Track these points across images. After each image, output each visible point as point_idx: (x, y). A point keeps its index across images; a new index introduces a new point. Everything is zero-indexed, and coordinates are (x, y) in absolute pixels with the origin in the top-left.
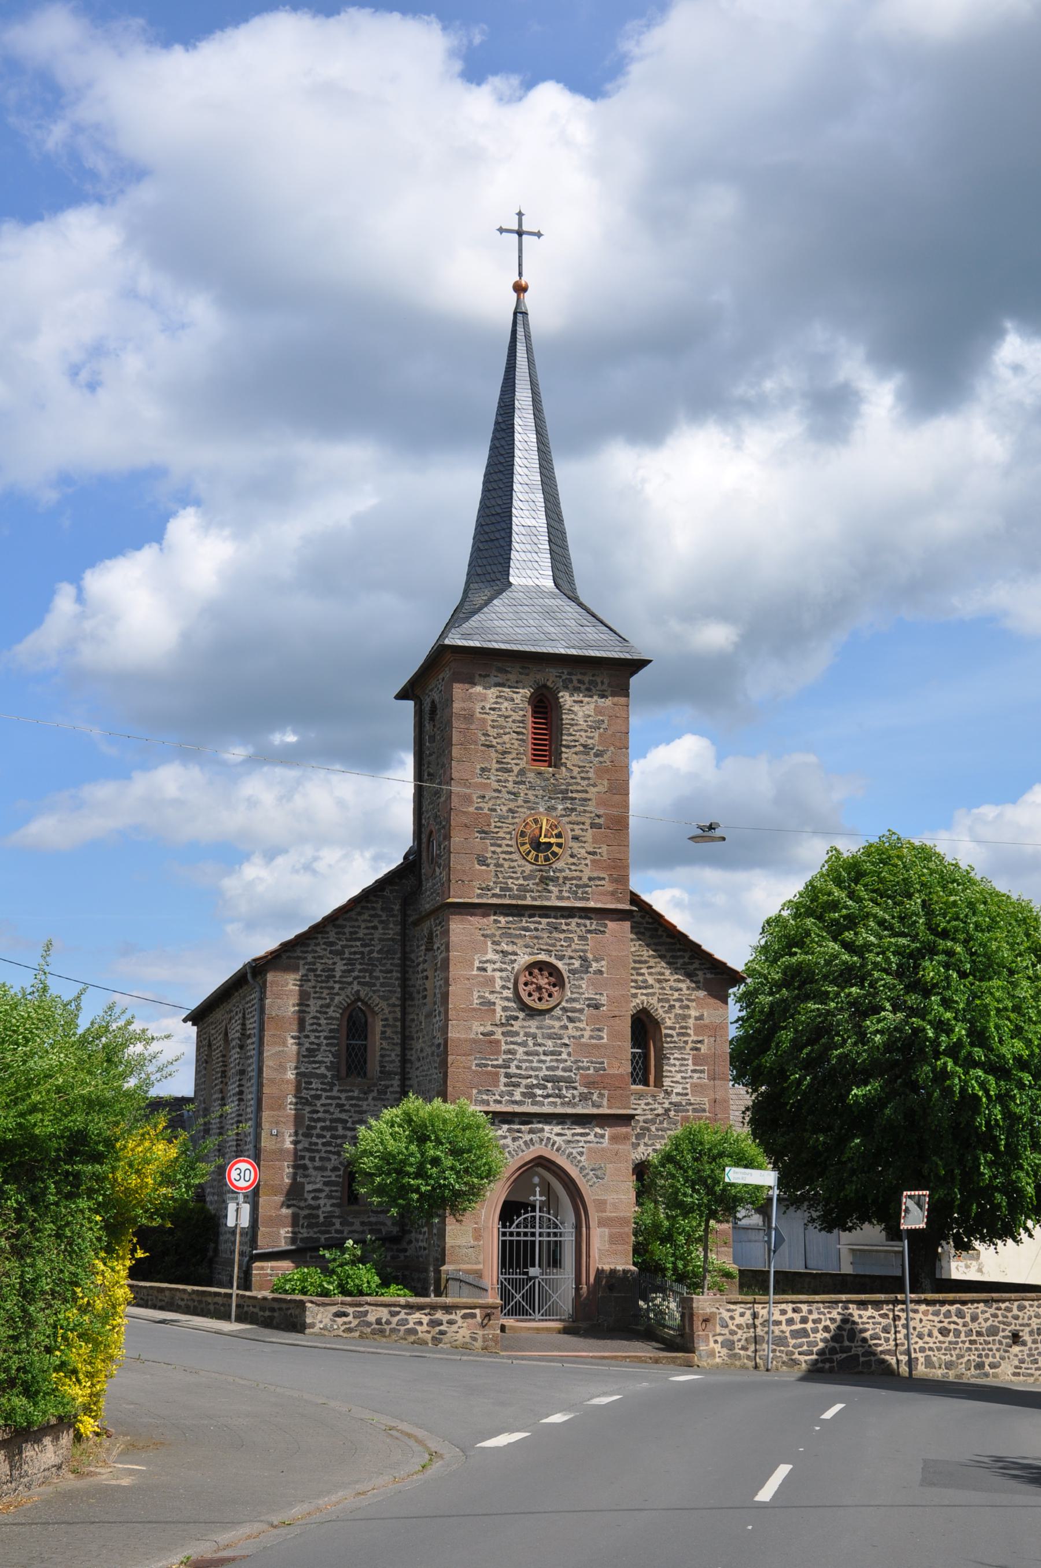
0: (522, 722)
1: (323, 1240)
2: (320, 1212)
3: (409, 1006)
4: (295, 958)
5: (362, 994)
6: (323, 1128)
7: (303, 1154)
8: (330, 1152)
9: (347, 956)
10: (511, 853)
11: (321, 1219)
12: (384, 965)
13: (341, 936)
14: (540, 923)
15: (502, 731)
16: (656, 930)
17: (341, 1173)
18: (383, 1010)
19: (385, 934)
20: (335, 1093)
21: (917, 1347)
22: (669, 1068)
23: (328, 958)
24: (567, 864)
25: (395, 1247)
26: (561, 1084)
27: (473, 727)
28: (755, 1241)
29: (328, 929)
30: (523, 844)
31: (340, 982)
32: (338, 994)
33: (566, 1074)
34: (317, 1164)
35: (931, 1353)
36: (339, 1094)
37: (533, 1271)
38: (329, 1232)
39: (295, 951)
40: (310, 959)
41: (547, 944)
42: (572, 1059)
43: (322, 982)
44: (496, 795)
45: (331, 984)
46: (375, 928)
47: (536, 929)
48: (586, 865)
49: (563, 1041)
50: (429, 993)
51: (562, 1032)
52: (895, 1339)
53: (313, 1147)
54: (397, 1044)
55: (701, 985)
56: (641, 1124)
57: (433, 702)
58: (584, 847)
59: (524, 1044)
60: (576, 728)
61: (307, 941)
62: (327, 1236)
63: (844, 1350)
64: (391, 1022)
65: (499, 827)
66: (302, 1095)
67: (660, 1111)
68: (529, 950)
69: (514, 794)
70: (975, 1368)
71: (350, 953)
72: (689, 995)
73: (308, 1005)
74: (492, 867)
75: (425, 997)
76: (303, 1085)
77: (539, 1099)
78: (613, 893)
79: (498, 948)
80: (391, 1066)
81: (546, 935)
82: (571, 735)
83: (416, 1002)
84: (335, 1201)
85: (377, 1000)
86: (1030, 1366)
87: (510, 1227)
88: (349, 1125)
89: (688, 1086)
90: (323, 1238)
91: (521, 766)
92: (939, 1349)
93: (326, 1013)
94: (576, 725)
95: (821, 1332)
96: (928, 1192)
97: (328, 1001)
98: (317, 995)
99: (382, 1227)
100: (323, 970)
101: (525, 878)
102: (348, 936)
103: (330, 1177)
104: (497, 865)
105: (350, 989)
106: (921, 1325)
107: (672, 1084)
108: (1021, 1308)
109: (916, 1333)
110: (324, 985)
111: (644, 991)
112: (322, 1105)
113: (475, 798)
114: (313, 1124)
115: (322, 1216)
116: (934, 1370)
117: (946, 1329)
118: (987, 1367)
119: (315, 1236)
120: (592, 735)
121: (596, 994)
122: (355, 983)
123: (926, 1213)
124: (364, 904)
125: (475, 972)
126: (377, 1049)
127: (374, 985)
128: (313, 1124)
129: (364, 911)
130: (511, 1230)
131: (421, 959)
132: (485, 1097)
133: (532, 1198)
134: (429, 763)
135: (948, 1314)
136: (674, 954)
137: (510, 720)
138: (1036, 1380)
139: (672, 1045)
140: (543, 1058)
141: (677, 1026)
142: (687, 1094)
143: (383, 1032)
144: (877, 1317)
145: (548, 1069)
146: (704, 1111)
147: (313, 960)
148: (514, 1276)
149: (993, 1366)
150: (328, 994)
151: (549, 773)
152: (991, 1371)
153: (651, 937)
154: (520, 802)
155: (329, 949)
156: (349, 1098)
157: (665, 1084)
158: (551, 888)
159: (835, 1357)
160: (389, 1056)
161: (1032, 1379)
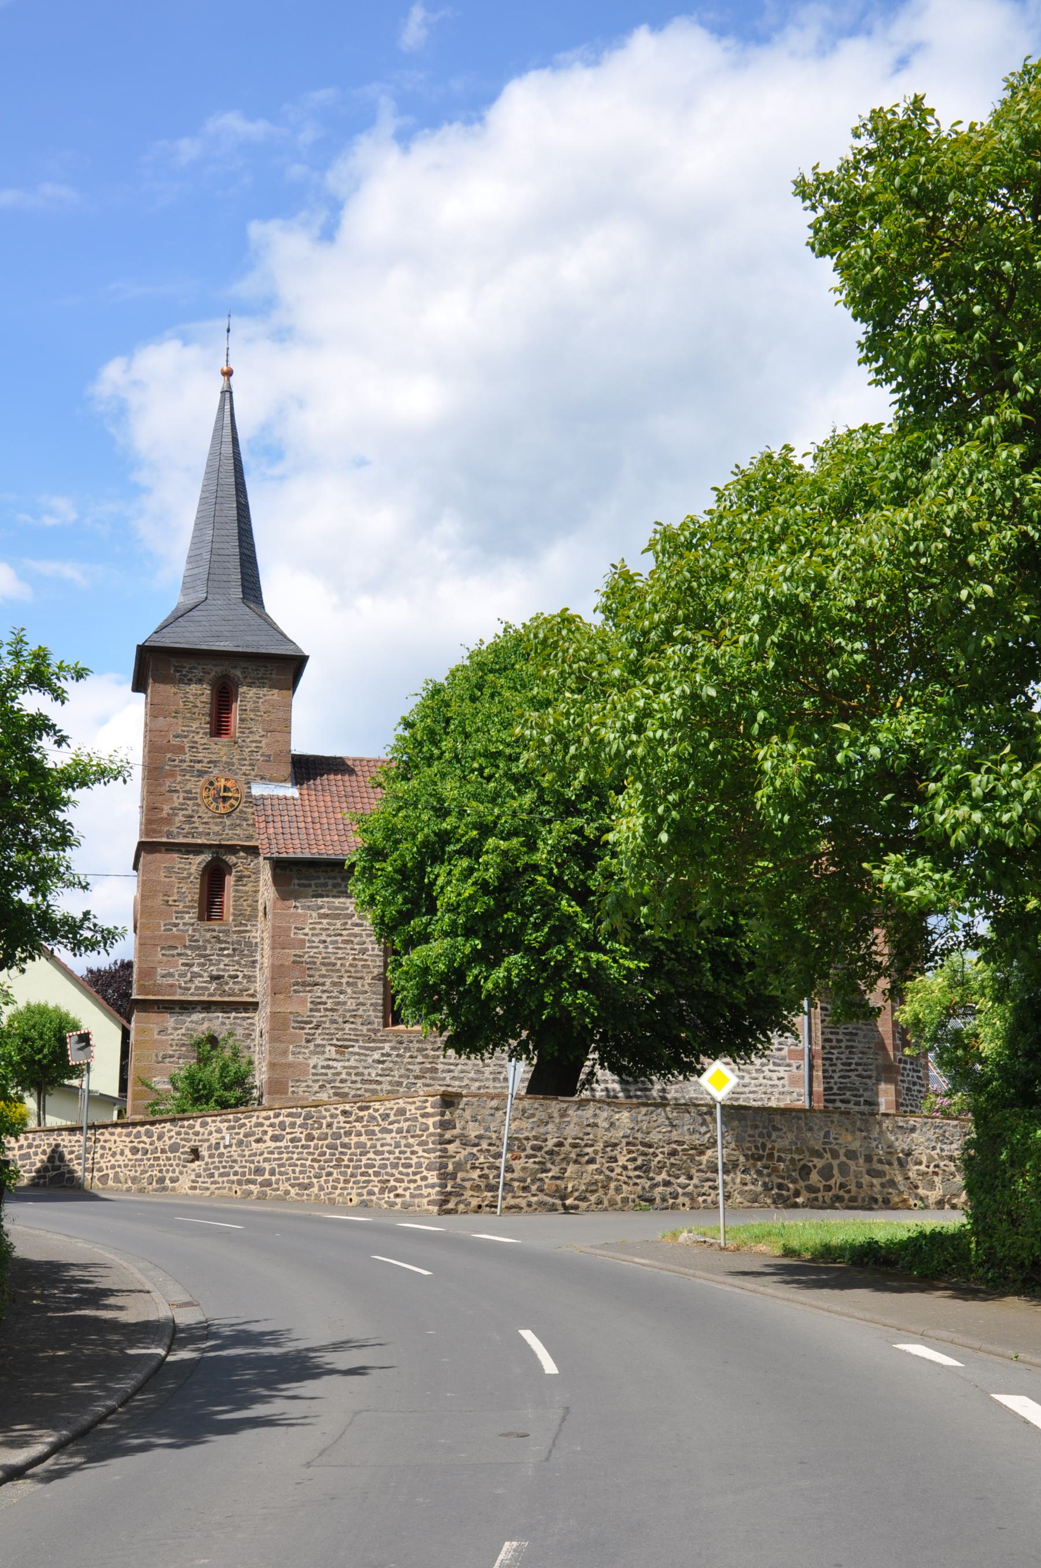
21: (109, 1165)
52: (93, 1159)
63: (54, 1169)
70: (157, 1183)
86: (206, 1180)
92: (126, 1166)
108: (204, 1125)
117: (135, 1147)
118: (167, 1182)
135: (138, 1135)
138: (212, 1193)
149: (174, 1180)
152: (170, 1185)
159: (48, 1174)
161: (208, 1193)
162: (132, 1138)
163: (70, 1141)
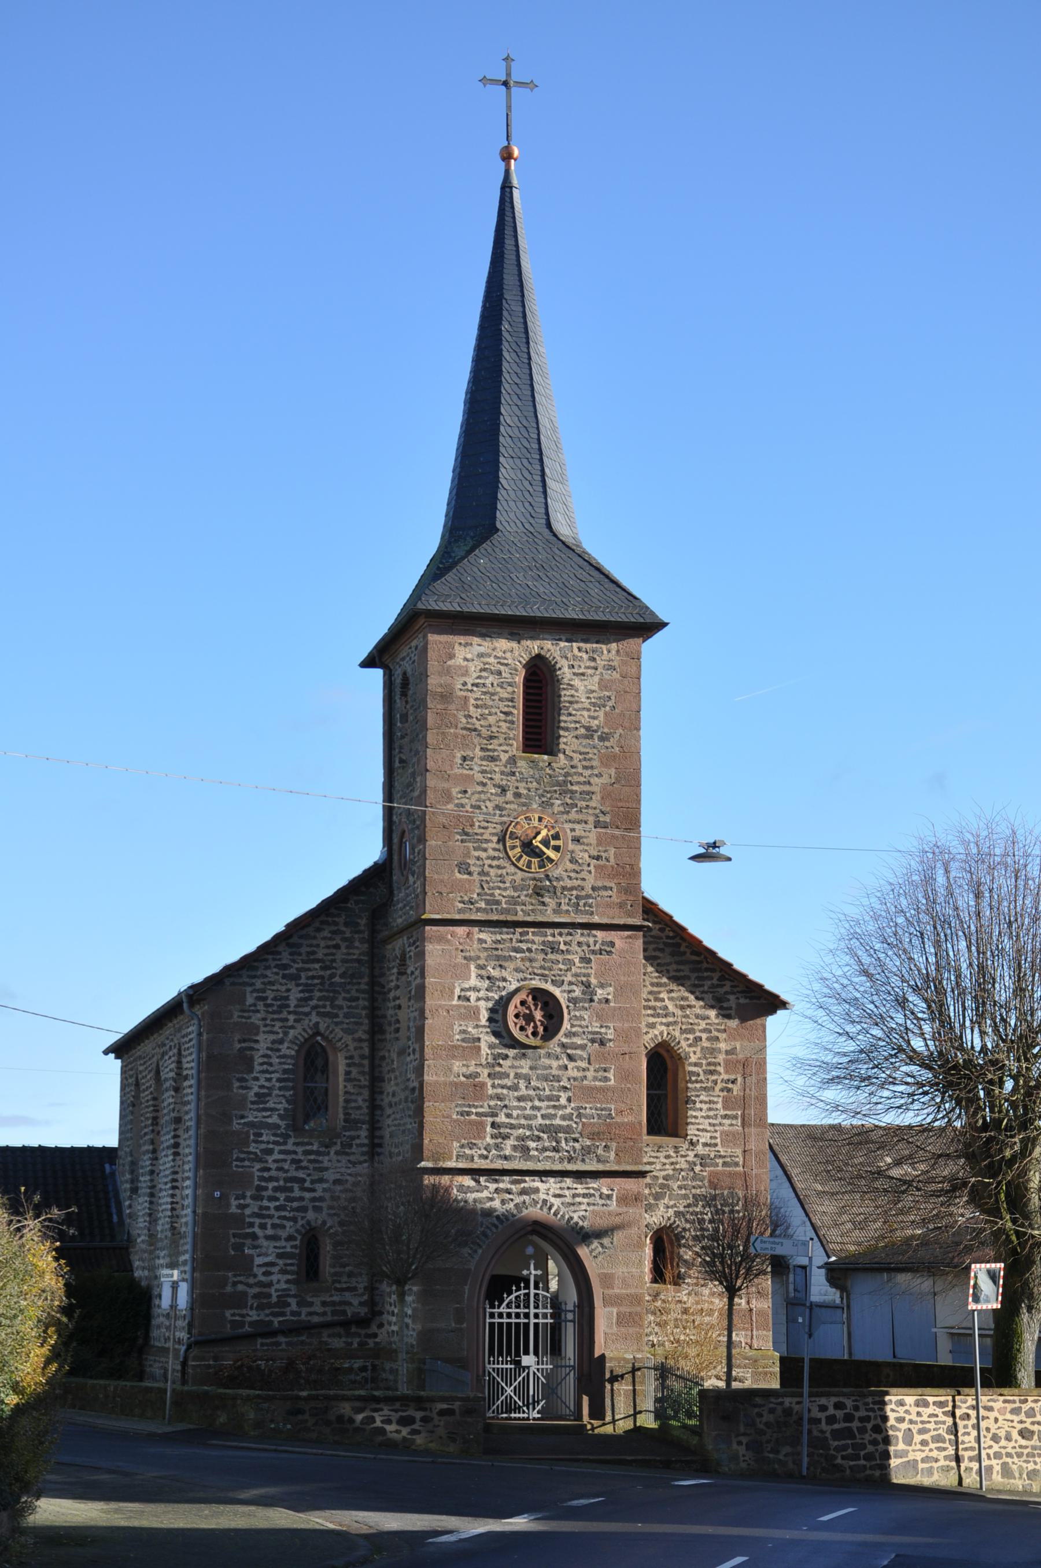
0: (512, 700)
1: (276, 1324)
2: (273, 1291)
3: (379, 1040)
4: (240, 984)
5: (322, 1027)
6: (276, 1189)
7: (252, 1220)
8: (284, 1218)
9: (303, 981)
10: (499, 858)
11: (274, 1299)
12: (348, 992)
13: (296, 957)
14: (533, 942)
15: (487, 712)
16: (679, 945)
17: (298, 1242)
18: (347, 1046)
19: (349, 954)
20: (289, 1147)
21: (991, 1452)
22: (694, 1114)
23: (281, 984)
24: (566, 871)
25: (363, 1332)
26: (560, 1135)
27: (452, 707)
28: (831, 1323)
29: (280, 948)
30: (513, 848)
31: (295, 1013)
32: (292, 1027)
33: (565, 1123)
34: (270, 1232)
35: (1009, 1460)
36: (294, 1148)
37: (528, 1360)
38: (283, 1314)
39: (241, 976)
40: (259, 985)
41: (542, 967)
42: (573, 1105)
43: (273, 1013)
44: (480, 788)
45: (284, 1015)
46: (337, 947)
47: (529, 950)
48: (590, 872)
49: (562, 1084)
50: (403, 1025)
51: (560, 1073)
53: (264, 1212)
54: (364, 1087)
55: (733, 1012)
56: (661, 1181)
57: (405, 673)
58: (586, 851)
59: (515, 1088)
60: (576, 706)
61: (256, 964)
62: (281, 1319)
64: (357, 1060)
65: (483, 828)
66: (251, 1149)
67: (684, 1166)
68: (520, 975)
69: (499, 786)
71: (308, 978)
72: (718, 1024)
73: (257, 1041)
74: (476, 876)
75: (397, 1030)
76: (252, 1137)
77: (532, 1153)
78: (621, 905)
79: (483, 973)
80: (358, 1112)
81: (541, 956)
82: (570, 715)
83: (388, 1036)
84: (290, 1277)
85: (341, 1034)
87: (499, 1307)
88: (307, 1185)
89: (718, 1135)
90: (276, 1321)
91: (510, 754)
93: (279, 1050)
94: (577, 702)
95: (870, 1432)
96: (1003, 1265)
97: (281, 1035)
98: (268, 1029)
99: (347, 1308)
100: (275, 999)
101: (515, 889)
102: (304, 957)
103: (285, 1247)
104: (482, 873)
105: (307, 1022)
106: (996, 1426)
107: (697, 1133)
109: (990, 1435)
110: (275, 1016)
111: (664, 1020)
112: (275, 1161)
113: (454, 794)
114: (263, 1184)
115: (274, 1295)
116: (1012, 1481)
119: (267, 1319)
120: (596, 714)
121: (601, 1027)
122: (314, 1013)
123: (1001, 1290)
124: (323, 918)
125: (455, 1002)
126: (341, 1093)
127: (337, 1016)
128: (263, 1184)
129: (325, 927)
130: (501, 1310)
131: (393, 984)
132: (468, 1151)
133: (525, 1272)
134: (401, 747)
136: (700, 974)
137: (496, 697)
139: (698, 1085)
140: (537, 1103)
141: (704, 1062)
142: (716, 1145)
143: (348, 1073)
144: (940, 1415)
145: (543, 1117)
146: (737, 1164)
147: (262, 986)
148: (505, 1366)
150: (281, 1027)
151: (544, 761)
153: (672, 954)
154: (509, 796)
155: (281, 972)
156: (307, 1153)
157: (689, 1132)
158: (547, 900)
160: (356, 1101)
162: (1023, 1417)
163: (919, 1414)
